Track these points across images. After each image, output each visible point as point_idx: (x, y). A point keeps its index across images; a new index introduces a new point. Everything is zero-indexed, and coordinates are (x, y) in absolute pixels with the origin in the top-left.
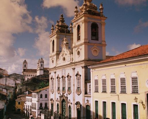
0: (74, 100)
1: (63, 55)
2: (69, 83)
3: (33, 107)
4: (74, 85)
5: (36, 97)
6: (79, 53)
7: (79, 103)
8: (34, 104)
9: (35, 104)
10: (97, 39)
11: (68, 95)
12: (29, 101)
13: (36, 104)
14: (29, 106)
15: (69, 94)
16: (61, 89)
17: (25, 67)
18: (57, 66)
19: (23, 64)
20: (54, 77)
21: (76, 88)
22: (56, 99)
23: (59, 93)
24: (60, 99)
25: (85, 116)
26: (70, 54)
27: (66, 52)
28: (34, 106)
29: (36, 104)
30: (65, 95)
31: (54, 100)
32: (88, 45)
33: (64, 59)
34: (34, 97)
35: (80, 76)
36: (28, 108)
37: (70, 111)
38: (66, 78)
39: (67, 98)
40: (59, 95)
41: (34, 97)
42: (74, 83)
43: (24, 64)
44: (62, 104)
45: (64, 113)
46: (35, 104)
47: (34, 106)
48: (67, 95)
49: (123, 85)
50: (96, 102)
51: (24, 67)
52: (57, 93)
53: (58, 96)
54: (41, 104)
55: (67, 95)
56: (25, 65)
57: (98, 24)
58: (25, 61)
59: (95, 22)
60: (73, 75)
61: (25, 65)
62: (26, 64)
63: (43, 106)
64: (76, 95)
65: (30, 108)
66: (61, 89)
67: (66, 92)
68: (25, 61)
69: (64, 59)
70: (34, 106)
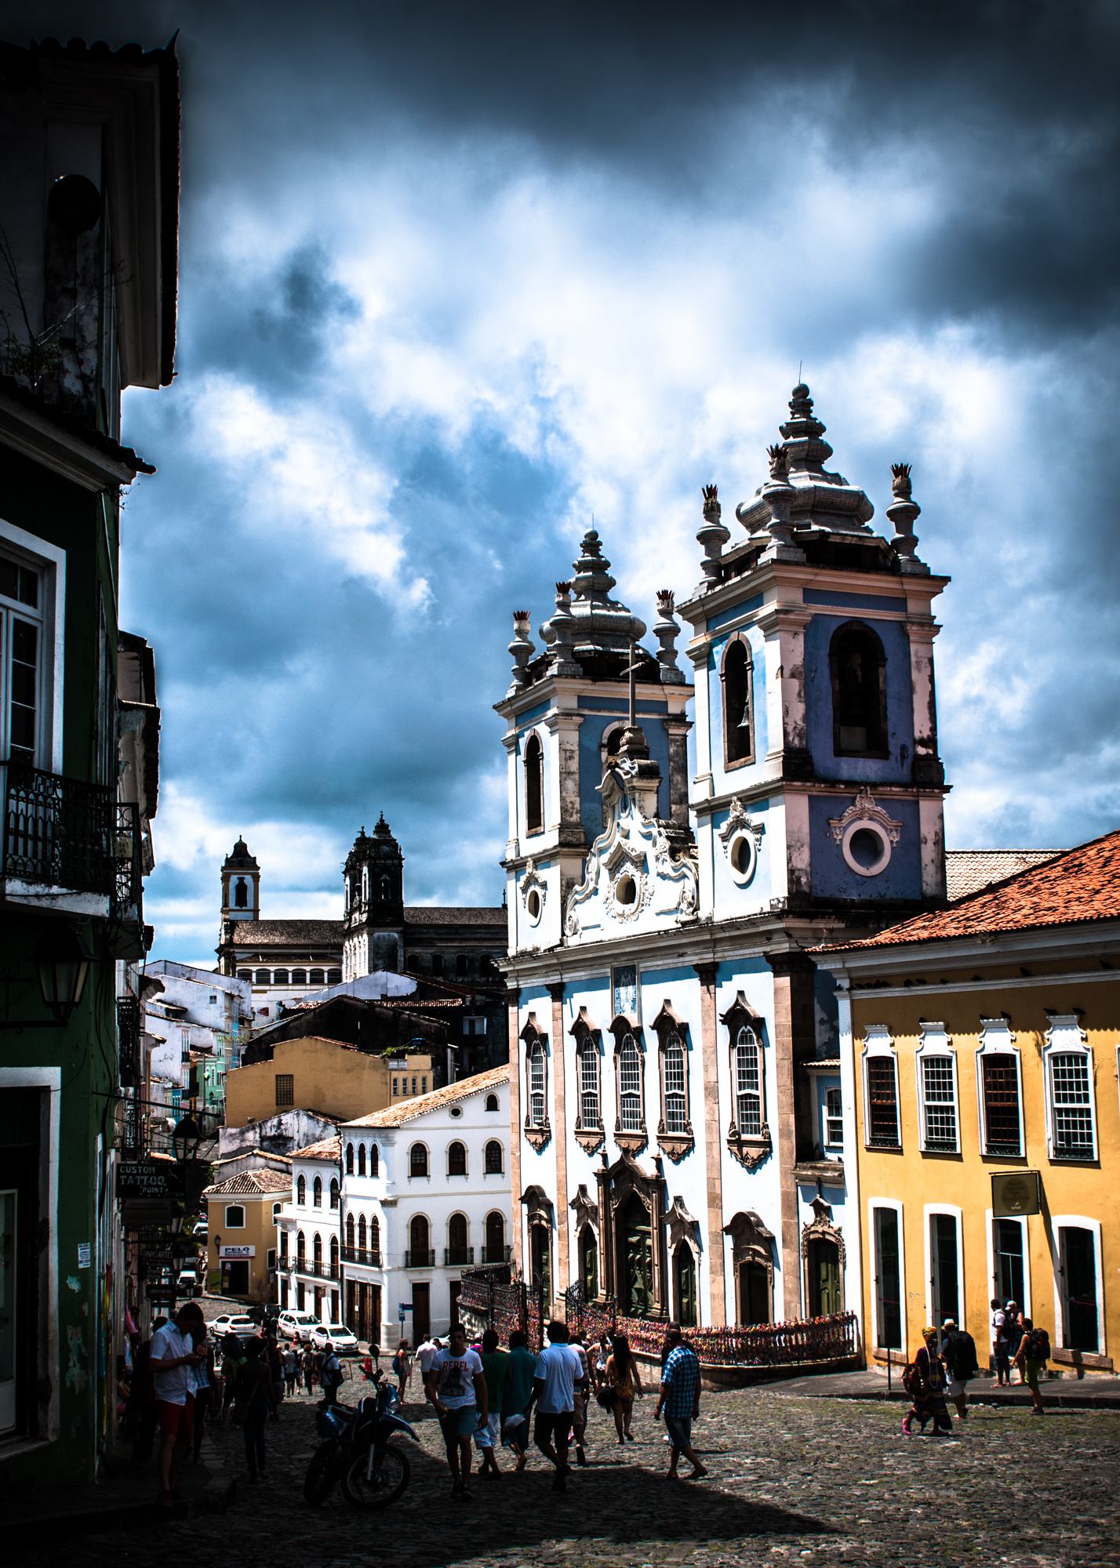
0: (715, 1201)
1: (614, 867)
2: (676, 1076)
3: (357, 1245)
4: (712, 1091)
5: (375, 1173)
6: (742, 857)
8: (362, 1226)
9: (369, 1223)
11: (667, 1163)
13: (375, 1220)
14: (317, 1238)
15: (678, 1158)
16: (609, 1112)
17: (241, 900)
18: (573, 941)
19: (225, 879)
20: (544, 1024)
21: (727, 1112)
22: (573, 1194)
23: (591, 1151)
24: (607, 1196)
26: (673, 853)
27: (637, 845)
28: (363, 1243)
30: (645, 1164)
31: (552, 1195)
32: (810, 797)
33: (628, 892)
34: (362, 1172)
35: (759, 1024)
36: (309, 1254)
37: (686, 1288)
38: (652, 1039)
39: (659, 1185)
40: (596, 1164)
41: (362, 1172)
42: (712, 1070)
43: (234, 880)
44: (625, 1230)
45: (635, 1297)
46: (369, 1223)
48: (659, 1162)
49: (1068, 1105)
50: (886, 1222)
51: (232, 904)
52: (575, 1150)
53: (584, 1170)
54: (419, 1226)
55: (659, 1162)
56: (241, 889)
57: (875, 627)
58: (241, 848)
60: (705, 1013)
61: (241, 889)
62: (248, 880)
63: (439, 1239)
64: (731, 1166)
66: (609, 1112)
68: (241, 848)
69: (628, 892)
70: (363, 1243)
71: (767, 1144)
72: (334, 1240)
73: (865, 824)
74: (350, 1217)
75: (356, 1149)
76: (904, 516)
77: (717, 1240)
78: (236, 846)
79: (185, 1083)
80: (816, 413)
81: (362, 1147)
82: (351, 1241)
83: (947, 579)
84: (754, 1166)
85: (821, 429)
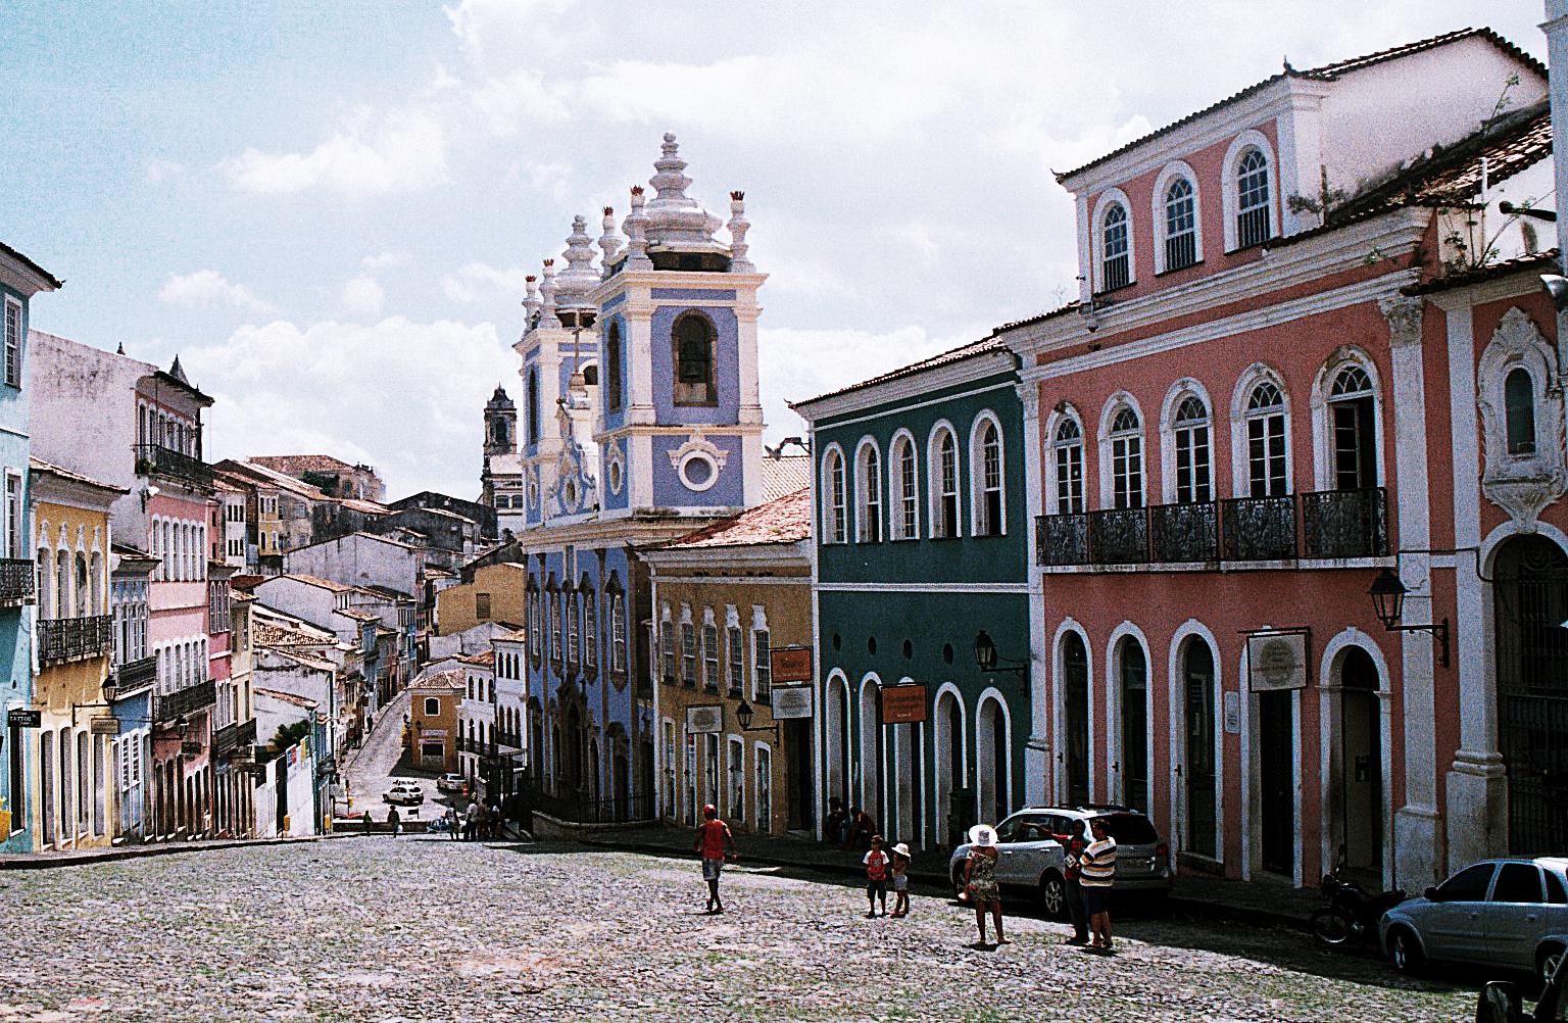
5: (517, 677)
7: (622, 730)
9: (514, 714)
10: (712, 400)
12: (481, 699)
13: (517, 710)
23: (558, 673)
25: (639, 789)
28: (510, 729)
29: (517, 710)
34: (509, 676)
36: (477, 738)
39: (584, 699)
41: (509, 676)
46: (514, 714)
47: (510, 723)
48: (583, 682)
59: (695, 309)
65: (487, 741)
67: (582, 669)
71: (626, 673)
72: (491, 726)
73: (698, 454)
74: (501, 708)
75: (505, 657)
76: (739, 229)
77: (606, 742)
78: (496, 392)
79: (419, 598)
80: (682, 155)
81: (509, 656)
82: (502, 723)
83: (764, 277)
84: (620, 689)
85: (681, 166)
